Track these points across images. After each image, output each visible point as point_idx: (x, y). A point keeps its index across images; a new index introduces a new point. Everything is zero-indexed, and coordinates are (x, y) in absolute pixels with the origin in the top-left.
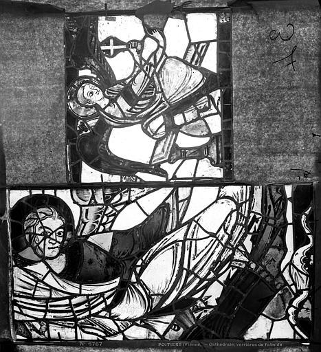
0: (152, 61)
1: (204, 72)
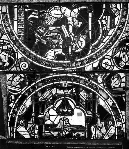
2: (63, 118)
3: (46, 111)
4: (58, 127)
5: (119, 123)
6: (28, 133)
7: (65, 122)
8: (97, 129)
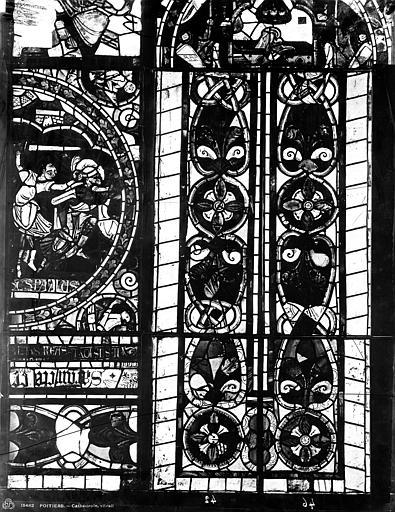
0: (107, 5)
1: (96, 46)
2: (270, 28)
3: (235, 15)
4: (258, 47)
5: (379, 39)
6: (198, 58)
7: (272, 36)
8: (336, 50)
